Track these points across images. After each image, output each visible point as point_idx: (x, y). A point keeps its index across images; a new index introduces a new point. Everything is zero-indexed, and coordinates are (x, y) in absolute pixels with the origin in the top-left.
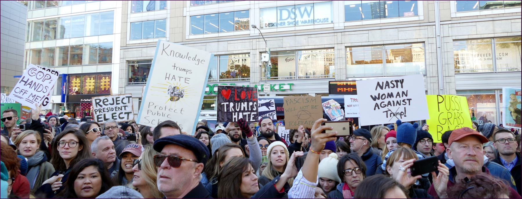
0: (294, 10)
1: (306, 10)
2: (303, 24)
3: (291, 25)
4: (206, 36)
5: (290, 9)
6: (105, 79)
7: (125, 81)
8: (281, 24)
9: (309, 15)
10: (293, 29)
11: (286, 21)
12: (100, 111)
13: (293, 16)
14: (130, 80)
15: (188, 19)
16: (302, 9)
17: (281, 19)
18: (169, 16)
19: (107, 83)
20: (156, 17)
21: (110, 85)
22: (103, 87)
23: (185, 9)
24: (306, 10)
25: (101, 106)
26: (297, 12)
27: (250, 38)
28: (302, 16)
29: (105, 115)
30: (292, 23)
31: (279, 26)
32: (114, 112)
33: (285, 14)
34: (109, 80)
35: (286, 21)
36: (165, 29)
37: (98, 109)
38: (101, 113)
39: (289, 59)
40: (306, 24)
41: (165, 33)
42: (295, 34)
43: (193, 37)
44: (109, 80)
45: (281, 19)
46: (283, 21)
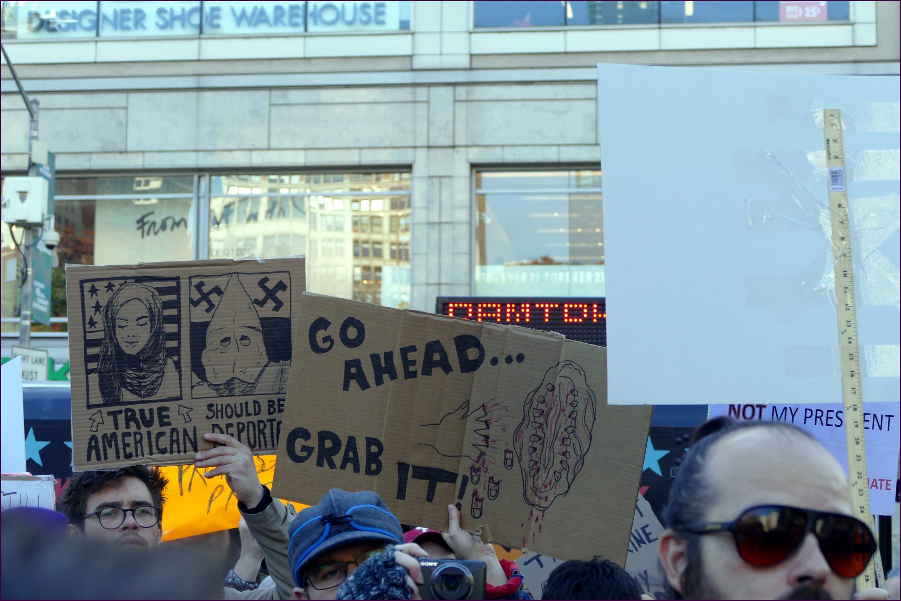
2: (246, 29)
3: (178, 30)
10: (187, 50)
30: (184, 18)
31: (107, 31)
40: (263, 29)
42: (199, 82)
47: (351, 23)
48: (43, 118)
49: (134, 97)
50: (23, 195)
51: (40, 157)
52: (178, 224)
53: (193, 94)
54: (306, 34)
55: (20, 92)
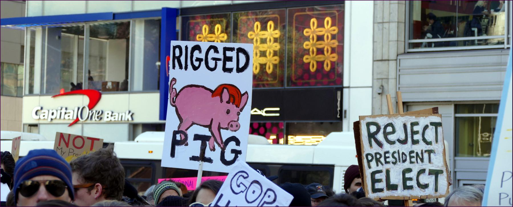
6: (321, 25)
7: (396, 33)
12: (378, 161)
14: (417, 30)
19: (327, 44)
21: (339, 51)
22: (311, 60)
25: (380, 145)
29: (388, 172)
32: (407, 165)
34: (335, 30)
37: (373, 152)
38: (380, 167)
44: (335, 30)
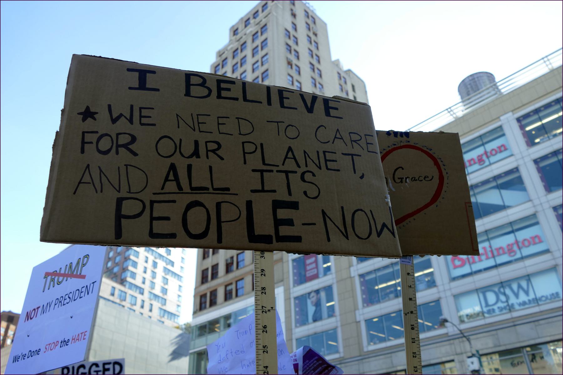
0: (502, 290)
1: (520, 287)
2: (522, 307)
3: (504, 311)
4: (389, 344)
5: (496, 289)
8: (489, 312)
9: (527, 293)
10: (508, 316)
11: (495, 307)
13: (503, 298)
15: (363, 326)
16: (515, 286)
17: (487, 305)
18: (339, 324)
20: (325, 328)
23: (357, 312)
24: (520, 287)
26: (508, 291)
27: (448, 339)
28: (517, 295)
30: (505, 308)
33: (491, 298)
35: (495, 307)
36: (336, 341)
39: (516, 362)
40: (527, 306)
41: (336, 347)
42: (514, 323)
43: (372, 347)
45: (487, 305)
46: (491, 308)
47: (551, 299)
48: (472, 342)
49: (499, 331)
50: (472, 363)
51: (474, 352)
52: (521, 363)
53: (513, 328)
54: (539, 305)
55: (464, 336)
